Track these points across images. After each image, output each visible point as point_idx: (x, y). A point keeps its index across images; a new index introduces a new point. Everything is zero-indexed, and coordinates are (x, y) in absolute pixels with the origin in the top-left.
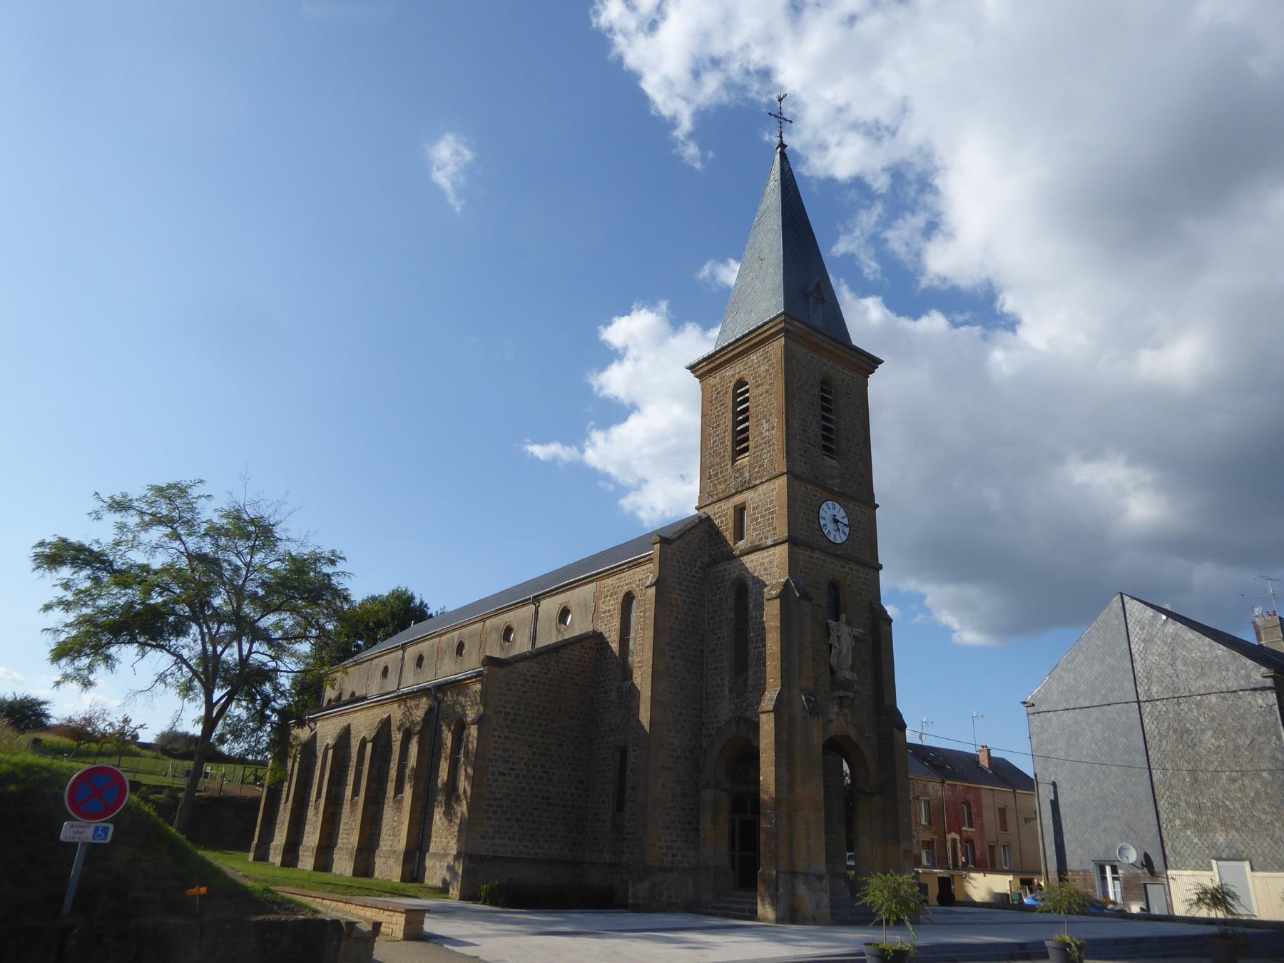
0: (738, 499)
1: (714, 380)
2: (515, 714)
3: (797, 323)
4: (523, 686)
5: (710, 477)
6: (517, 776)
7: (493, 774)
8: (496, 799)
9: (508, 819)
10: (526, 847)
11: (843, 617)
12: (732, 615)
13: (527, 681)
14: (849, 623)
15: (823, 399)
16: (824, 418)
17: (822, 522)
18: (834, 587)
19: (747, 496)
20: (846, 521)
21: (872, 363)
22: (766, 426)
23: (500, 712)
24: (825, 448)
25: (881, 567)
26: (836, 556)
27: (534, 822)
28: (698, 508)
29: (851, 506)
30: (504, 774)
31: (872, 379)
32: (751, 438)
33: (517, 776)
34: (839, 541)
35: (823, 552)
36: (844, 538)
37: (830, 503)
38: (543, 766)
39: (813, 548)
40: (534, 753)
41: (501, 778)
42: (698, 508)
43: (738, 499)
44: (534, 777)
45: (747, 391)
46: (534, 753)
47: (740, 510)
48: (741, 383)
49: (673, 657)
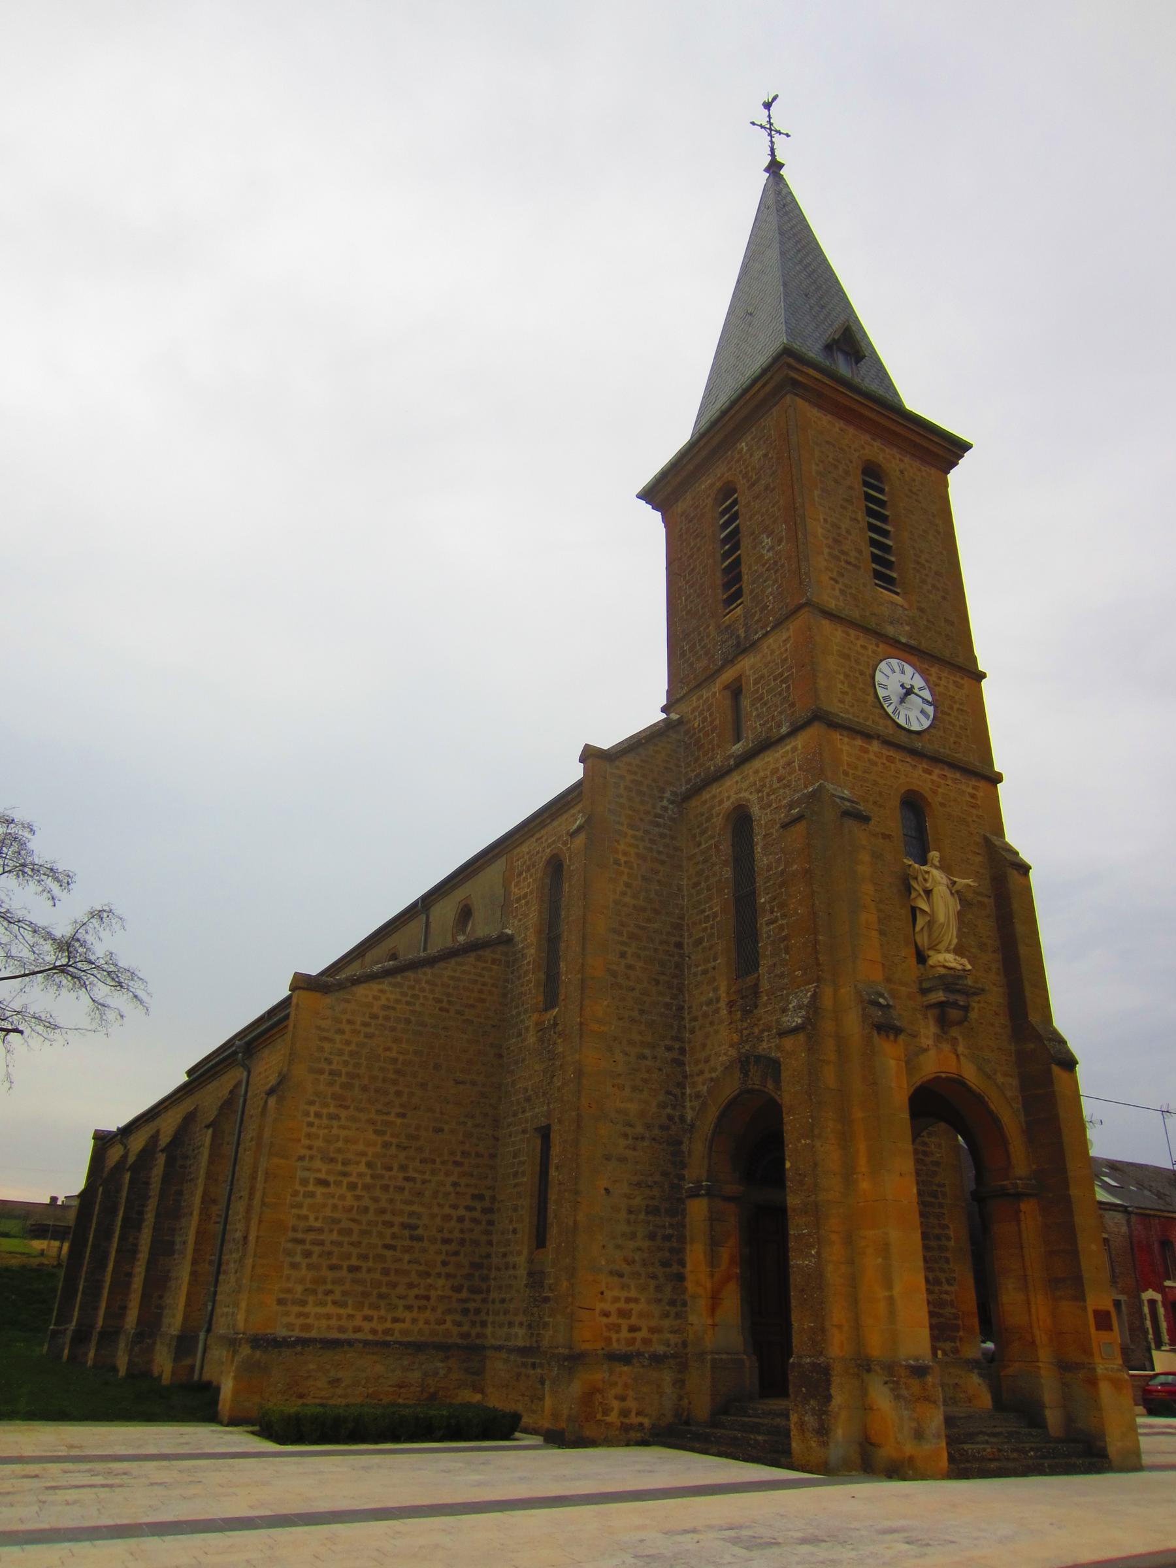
0: (728, 675)
1: (680, 507)
2: (351, 1076)
3: (811, 372)
4: (365, 1025)
5: (683, 654)
6: (352, 1186)
7: (304, 1182)
8: (310, 1230)
9: (332, 1268)
10: (368, 1318)
11: (934, 855)
12: (728, 873)
13: (375, 1017)
14: (944, 867)
15: (868, 498)
16: (872, 528)
17: (881, 693)
18: (914, 805)
19: (748, 664)
20: (926, 694)
21: (946, 450)
22: (767, 541)
23: (321, 1072)
24: (877, 575)
25: (998, 778)
26: (913, 752)
27: (386, 1272)
28: (664, 710)
29: (933, 670)
30: (324, 1183)
31: (954, 477)
32: (746, 591)
33: (352, 1186)
34: (916, 727)
35: (887, 743)
36: (926, 724)
37: (894, 662)
38: (403, 1168)
39: (868, 736)
40: (386, 1145)
41: (320, 1190)
42: (664, 710)
43: (728, 675)
44: (386, 1188)
45: (735, 502)
46: (386, 1145)
47: (736, 691)
48: (728, 491)
49: (623, 955)
